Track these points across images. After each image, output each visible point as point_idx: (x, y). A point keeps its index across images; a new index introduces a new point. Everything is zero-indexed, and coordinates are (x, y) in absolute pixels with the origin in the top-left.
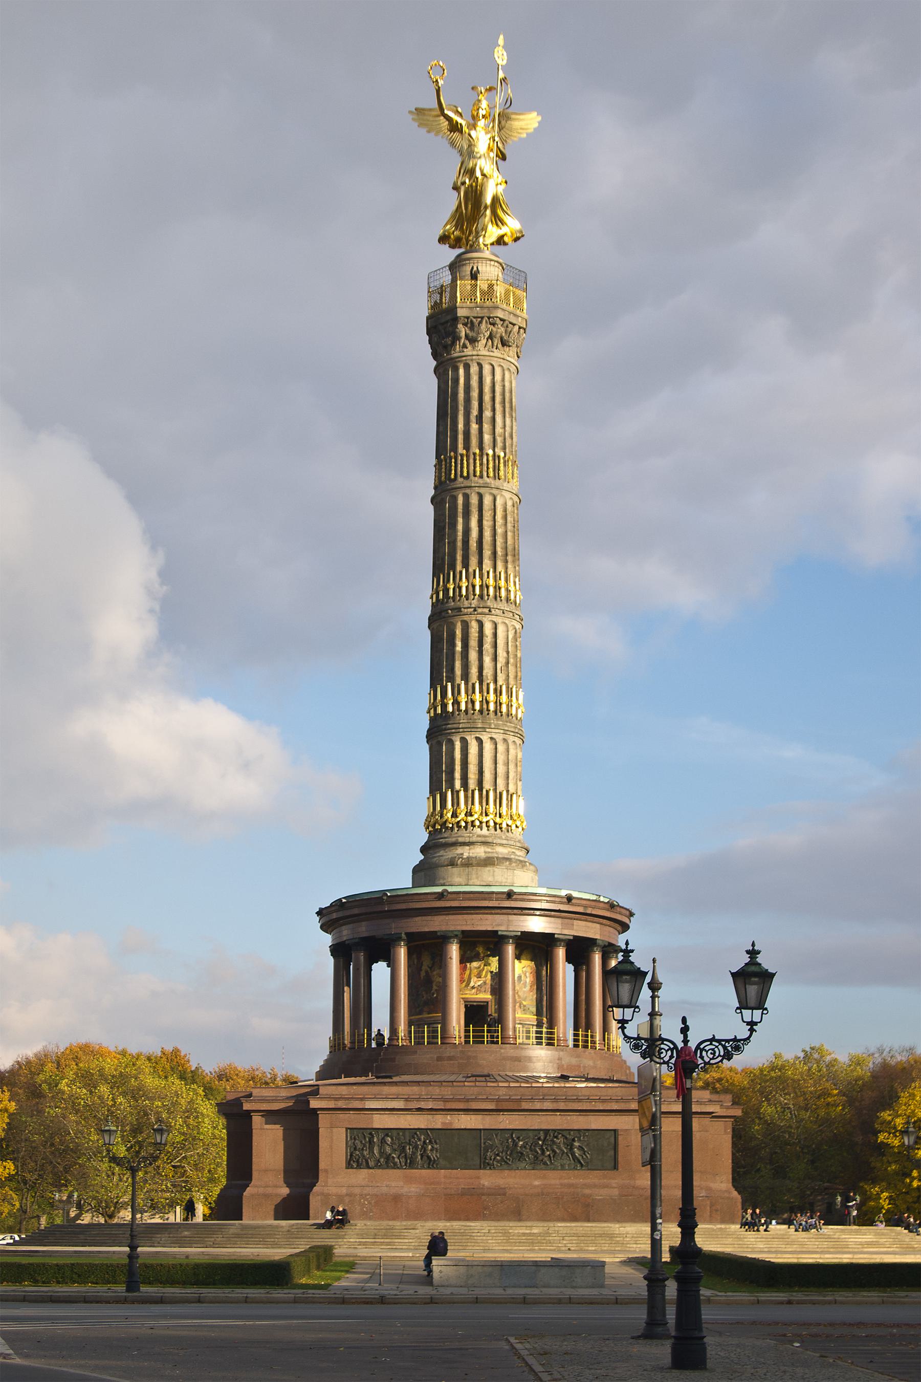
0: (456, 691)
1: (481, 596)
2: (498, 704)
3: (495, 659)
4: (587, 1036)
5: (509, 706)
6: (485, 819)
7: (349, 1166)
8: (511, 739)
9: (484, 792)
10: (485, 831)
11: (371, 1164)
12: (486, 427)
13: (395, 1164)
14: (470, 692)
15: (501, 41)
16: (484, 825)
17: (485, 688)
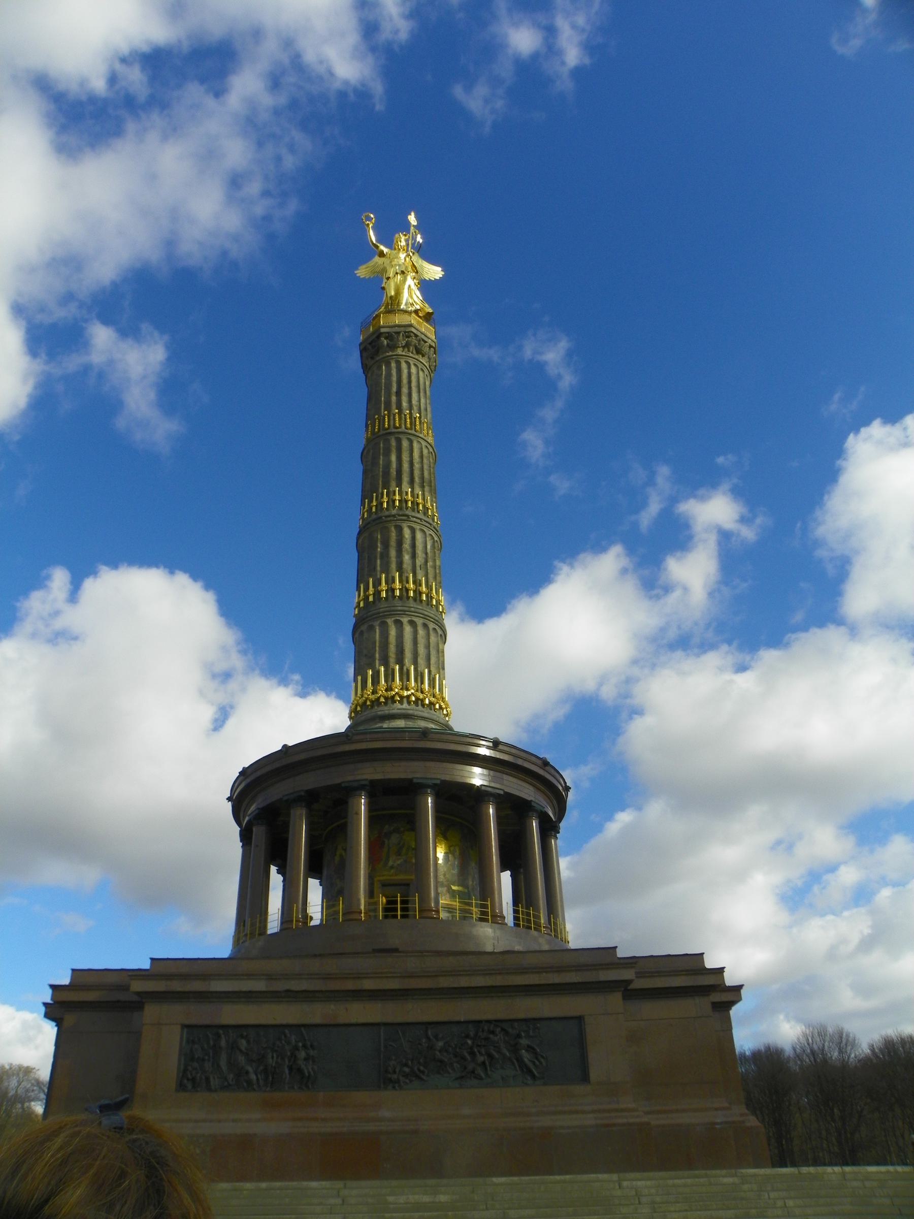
0: (377, 583)
1: (400, 508)
2: (418, 593)
3: (414, 556)
4: (528, 914)
5: (429, 597)
6: (406, 693)
7: (181, 1087)
8: (431, 626)
9: (405, 668)
10: (405, 705)
11: (215, 1082)
12: (404, 399)
13: (249, 1082)
14: (390, 581)
15: (413, 214)
16: (405, 700)
17: (404, 578)
